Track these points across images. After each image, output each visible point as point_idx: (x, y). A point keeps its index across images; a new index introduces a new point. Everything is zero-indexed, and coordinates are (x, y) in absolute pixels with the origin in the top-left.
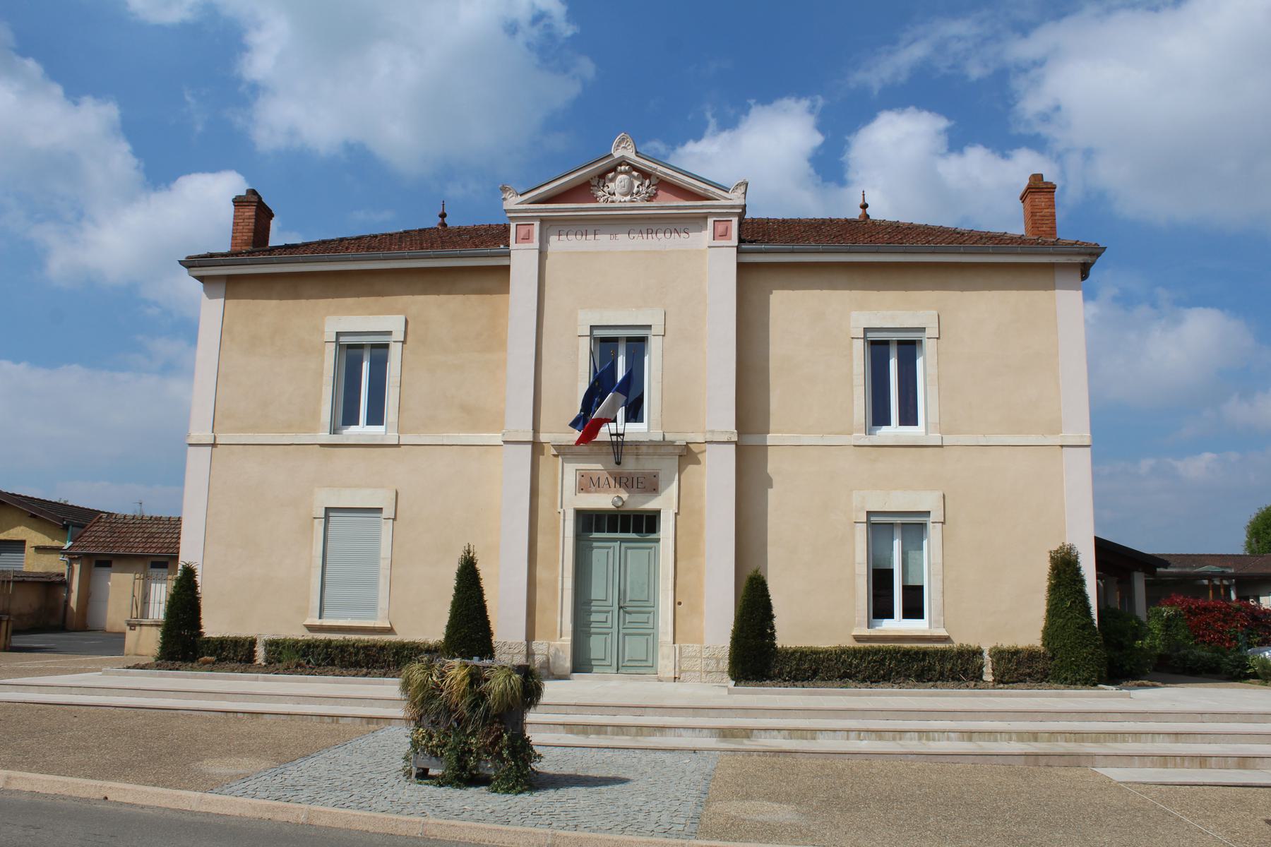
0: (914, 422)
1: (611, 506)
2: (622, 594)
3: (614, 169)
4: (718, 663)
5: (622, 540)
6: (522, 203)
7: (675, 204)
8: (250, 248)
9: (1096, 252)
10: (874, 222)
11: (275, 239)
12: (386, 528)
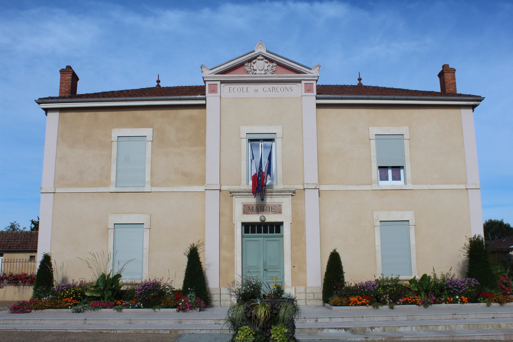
0: (399, 179)
1: (259, 221)
2: (265, 264)
3: (255, 58)
4: (314, 295)
5: (264, 237)
7: (286, 75)
8: (67, 95)
9: (480, 99)
10: (366, 86)
11: (79, 92)
12: (147, 234)
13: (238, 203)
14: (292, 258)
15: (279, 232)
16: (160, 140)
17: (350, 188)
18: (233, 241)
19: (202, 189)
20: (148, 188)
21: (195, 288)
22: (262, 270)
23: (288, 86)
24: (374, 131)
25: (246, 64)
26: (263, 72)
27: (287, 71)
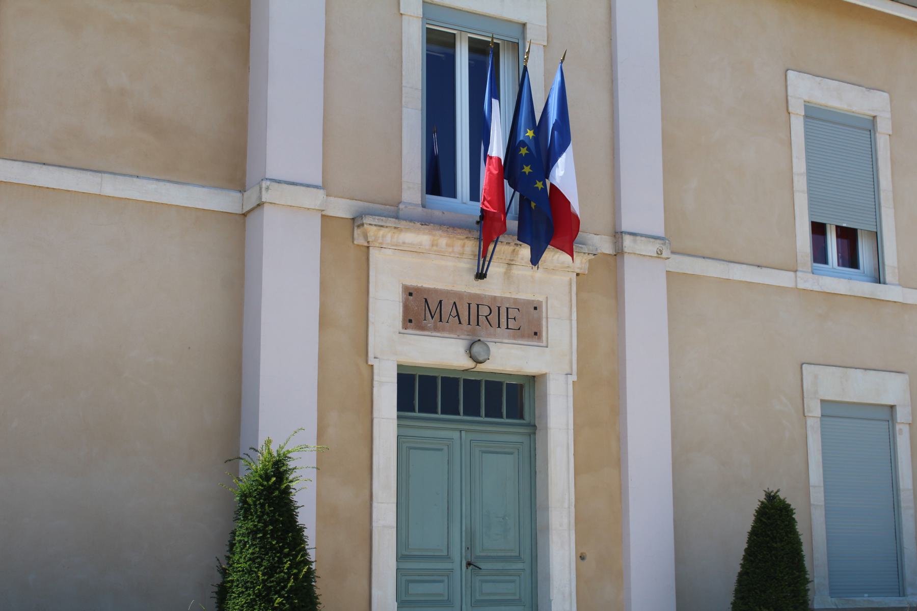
14: (579, 520)
17: (739, 273)
24: (805, 89)
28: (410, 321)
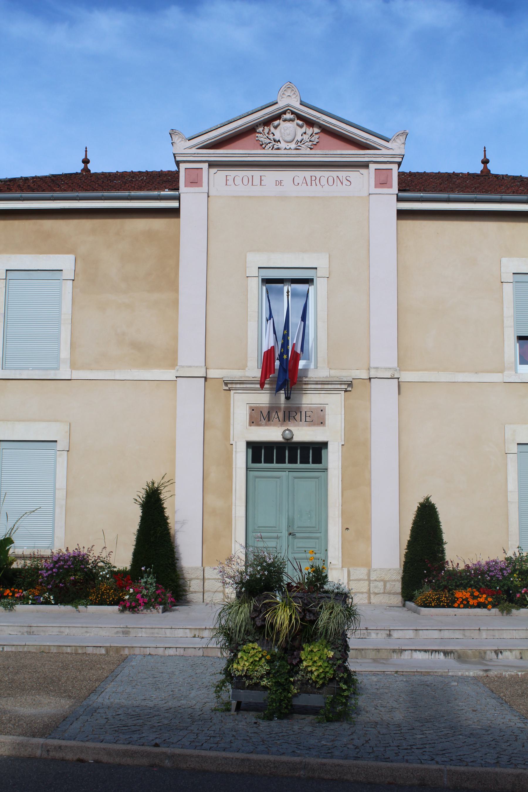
2: (290, 523)
3: (278, 117)
4: (385, 586)
5: (291, 470)
6: (191, 148)
7: (339, 152)
10: (497, 176)
12: (62, 460)
13: (241, 404)
15: (320, 462)
16: (88, 278)
17: (461, 377)
18: (230, 477)
19: (170, 375)
20: (65, 373)
21: (156, 567)
22: (285, 533)
23: (343, 174)
24: (511, 265)
25: (260, 129)
26: (293, 145)
27: (341, 143)
28: (253, 423)
